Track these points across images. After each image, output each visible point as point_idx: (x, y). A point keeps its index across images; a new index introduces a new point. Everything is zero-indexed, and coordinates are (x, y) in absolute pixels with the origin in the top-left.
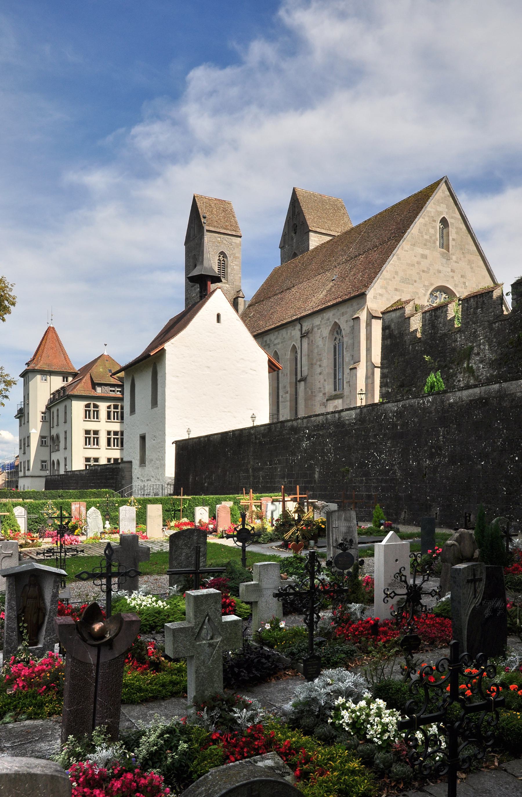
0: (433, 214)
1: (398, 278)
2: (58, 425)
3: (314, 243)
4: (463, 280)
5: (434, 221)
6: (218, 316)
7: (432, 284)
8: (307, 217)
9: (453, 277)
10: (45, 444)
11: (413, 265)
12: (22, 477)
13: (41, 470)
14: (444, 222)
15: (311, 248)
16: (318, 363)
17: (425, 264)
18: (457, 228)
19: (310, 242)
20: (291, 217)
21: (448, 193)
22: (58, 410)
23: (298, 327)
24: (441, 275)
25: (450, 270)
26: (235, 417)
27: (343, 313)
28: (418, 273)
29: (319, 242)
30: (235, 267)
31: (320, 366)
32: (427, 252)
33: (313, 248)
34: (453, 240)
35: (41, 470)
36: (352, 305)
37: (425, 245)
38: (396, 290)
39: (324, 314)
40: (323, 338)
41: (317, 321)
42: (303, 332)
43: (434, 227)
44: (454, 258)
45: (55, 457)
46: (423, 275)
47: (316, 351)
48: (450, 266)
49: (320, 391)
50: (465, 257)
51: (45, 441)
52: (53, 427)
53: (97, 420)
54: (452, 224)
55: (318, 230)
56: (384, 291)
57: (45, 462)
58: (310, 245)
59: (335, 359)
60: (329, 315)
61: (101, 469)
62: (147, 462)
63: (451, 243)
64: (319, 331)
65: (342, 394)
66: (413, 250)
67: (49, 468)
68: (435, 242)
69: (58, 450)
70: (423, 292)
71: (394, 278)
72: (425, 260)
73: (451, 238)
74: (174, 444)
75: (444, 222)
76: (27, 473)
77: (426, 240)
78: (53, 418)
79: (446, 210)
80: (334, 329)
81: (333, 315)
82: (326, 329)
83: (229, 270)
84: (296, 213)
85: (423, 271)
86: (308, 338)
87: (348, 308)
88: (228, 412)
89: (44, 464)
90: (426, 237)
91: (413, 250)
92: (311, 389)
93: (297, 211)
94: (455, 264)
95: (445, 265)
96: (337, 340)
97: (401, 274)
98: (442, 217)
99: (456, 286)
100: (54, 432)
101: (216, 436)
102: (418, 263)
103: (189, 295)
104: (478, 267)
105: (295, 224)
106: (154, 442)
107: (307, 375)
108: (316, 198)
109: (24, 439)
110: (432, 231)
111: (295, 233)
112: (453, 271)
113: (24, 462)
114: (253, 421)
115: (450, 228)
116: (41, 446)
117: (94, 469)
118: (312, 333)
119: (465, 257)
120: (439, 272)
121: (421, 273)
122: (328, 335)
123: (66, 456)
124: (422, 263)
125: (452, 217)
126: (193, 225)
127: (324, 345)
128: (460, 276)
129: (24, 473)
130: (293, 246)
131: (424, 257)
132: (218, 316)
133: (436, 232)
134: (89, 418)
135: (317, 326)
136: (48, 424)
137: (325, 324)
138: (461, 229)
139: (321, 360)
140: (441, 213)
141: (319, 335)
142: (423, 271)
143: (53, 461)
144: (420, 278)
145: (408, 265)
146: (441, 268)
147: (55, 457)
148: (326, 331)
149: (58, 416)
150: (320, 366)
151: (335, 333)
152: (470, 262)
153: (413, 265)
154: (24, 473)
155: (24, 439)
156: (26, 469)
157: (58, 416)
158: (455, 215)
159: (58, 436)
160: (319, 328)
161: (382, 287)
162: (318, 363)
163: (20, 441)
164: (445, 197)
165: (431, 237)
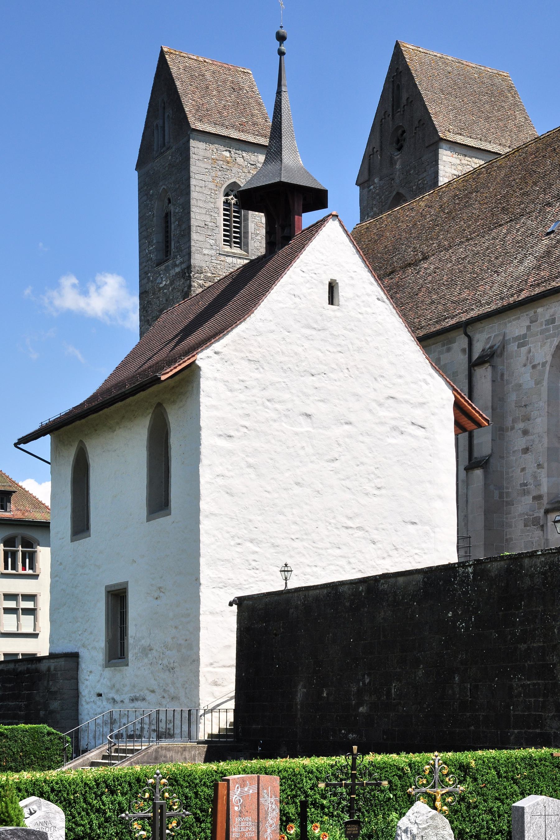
3: (448, 170)
8: (432, 109)
15: (443, 180)
16: (521, 425)
19: (441, 167)
23: (462, 342)
26: (374, 543)
29: (460, 168)
31: (525, 432)
33: (446, 180)
39: (540, 310)
40: (534, 367)
47: (513, 397)
55: (459, 139)
58: (441, 173)
74: (235, 607)
84: (404, 101)
86: (494, 367)
88: (359, 528)
93: (404, 96)
101: (401, 579)
105: (399, 127)
107: (490, 456)
108: (449, 69)
111: (400, 149)
114: (286, 579)
118: (502, 354)
137: (542, 332)
139: (527, 418)
160: (522, 341)
162: (521, 425)
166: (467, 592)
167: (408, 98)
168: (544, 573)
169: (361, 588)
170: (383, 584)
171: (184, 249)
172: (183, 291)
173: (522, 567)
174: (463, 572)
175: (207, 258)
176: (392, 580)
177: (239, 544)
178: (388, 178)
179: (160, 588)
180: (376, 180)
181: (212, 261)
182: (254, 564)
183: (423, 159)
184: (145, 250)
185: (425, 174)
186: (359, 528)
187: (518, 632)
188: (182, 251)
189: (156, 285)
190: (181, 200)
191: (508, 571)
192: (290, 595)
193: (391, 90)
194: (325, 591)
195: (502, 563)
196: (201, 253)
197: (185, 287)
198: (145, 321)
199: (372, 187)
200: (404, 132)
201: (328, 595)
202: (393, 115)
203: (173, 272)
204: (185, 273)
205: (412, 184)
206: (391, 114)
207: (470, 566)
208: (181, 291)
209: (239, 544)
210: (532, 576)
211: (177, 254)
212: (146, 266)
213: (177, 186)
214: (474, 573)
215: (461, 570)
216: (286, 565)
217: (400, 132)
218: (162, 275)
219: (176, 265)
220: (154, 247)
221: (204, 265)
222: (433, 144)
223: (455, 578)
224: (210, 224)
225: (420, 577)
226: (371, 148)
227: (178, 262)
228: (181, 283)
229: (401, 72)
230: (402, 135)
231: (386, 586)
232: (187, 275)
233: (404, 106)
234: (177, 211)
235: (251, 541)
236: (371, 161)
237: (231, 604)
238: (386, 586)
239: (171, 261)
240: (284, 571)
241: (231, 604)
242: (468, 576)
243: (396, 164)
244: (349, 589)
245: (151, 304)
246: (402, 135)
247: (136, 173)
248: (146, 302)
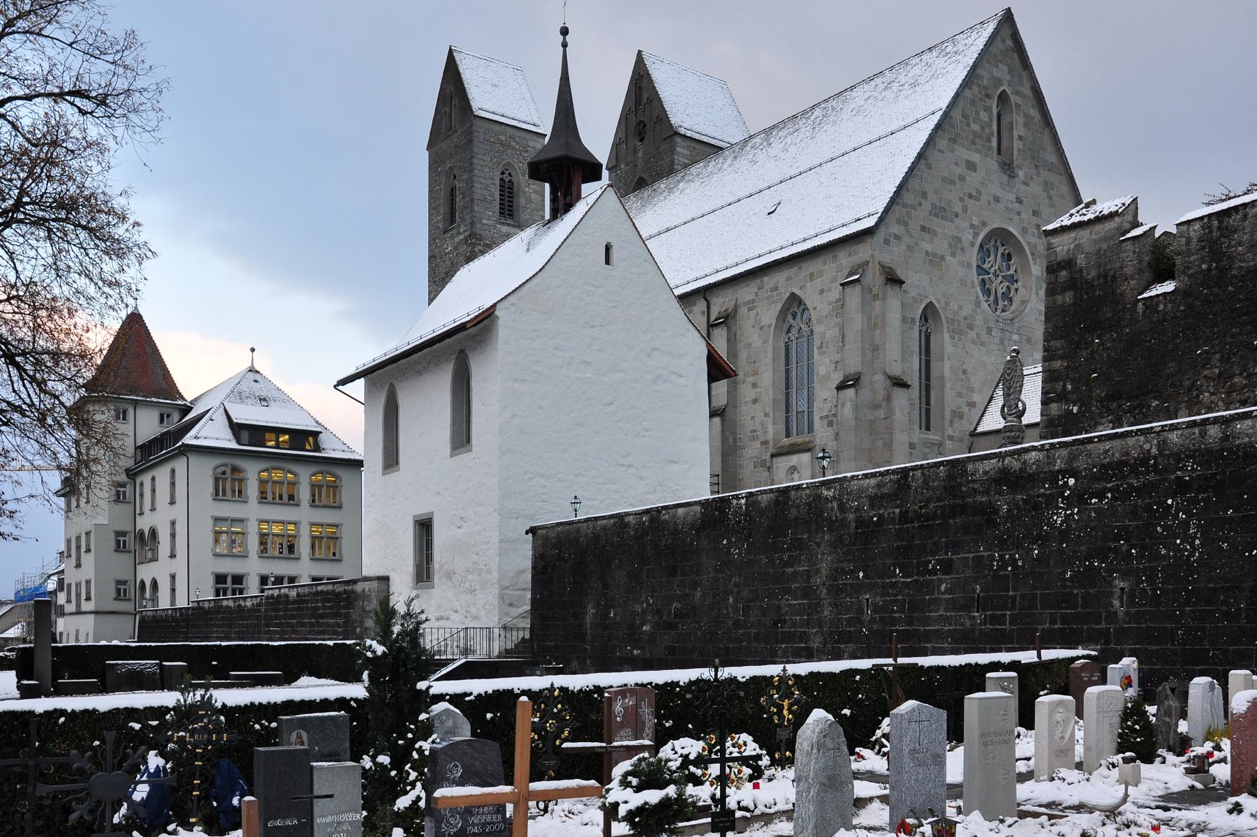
0: (985, 83)
1: (927, 206)
2: (153, 509)
4: (1035, 220)
5: (988, 96)
6: (608, 248)
7: (984, 224)
9: (1019, 213)
10: (124, 547)
11: (952, 182)
12: (72, 614)
13: (115, 599)
14: (1003, 97)
17: (973, 180)
18: (1026, 115)
20: (633, 109)
21: (1010, 43)
22: (153, 479)
24: (1000, 206)
25: (1013, 197)
27: (812, 275)
28: (961, 199)
30: (533, 196)
32: (976, 158)
34: (1020, 138)
35: (115, 599)
36: (835, 257)
37: (973, 143)
38: (924, 229)
41: (746, 293)
42: (713, 317)
43: (988, 109)
44: (1021, 174)
45: (146, 573)
46: (970, 203)
48: (1015, 190)
49: (754, 438)
50: (1038, 174)
51: (124, 541)
52: (142, 514)
53: (240, 499)
54: (1018, 106)
56: (902, 228)
57: (125, 583)
59: (787, 372)
60: (779, 278)
61: (298, 595)
62: (436, 578)
63: (1017, 145)
64: (753, 313)
65: (809, 442)
66: (952, 151)
67: (133, 597)
68: (989, 140)
69: (154, 559)
70: (970, 237)
71: (920, 204)
72: (974, 174)
73: (1016, 134)
74: (530, 535)
75: (1003, 97)
76: (86, 606)
77: (975, 133)
78: (142, 495)
79: (1008, 77)
80: (788, 310)
81: (788, 279)
82: (768, 310)
83: (522, 201)
84: (645, 100)
85: (970, 196)
87: (824, 263)
88: (630, 466)
89: (122, 587)
90: (975, 127)
91: (952, 151)
92: (734, 434)
93: (645, 95)
94: (1023, 187)
95: (1007, 189)
96: (794, 331)
97: (932, 197)
98: (1002, 89)
99: (1024, 231)
100: (144, 524)
101: (681, 511)
102: (962, 178)
103: (436, 251)
104: (1062, 196)
105: (641, 122)
106: (461, 531)
109: (78, 538)
110: (984, 116)
111: (641, 140)
112: (1019, 200)
113: (78, 585)
115: (1014, 115)
116: (116, 551)
117: (279, 596)
119: (1038, 174)
120: (997, 199)
121: (966, 199)
122: (774, 321)
123: (173, 571)
124: (968, 178)
125: (1018, 93)
126: (447, 109)
127: (765, 342)
128: (1030, 212)
129: (78, 605)
130: (636, 165)
131: (971, 166)
132: (608, 248)
133: (991, 120)
134: (224, 494)
135: (746, 303)
136: (129, 508)
138: (1032, 118)
140: (999, 82)
141: (751, 321)
142: (970, 196)
143: (143, 583)
144: (965, 210)
145: (944, 179)
146: (999, 193)
147: (146, 573)
148: (769, 315)
149: (153, 491)
150: (754, 385)
151: (790, 317)
152: (1047, 186)
153: (952, 182)
154: (78, 605)
155: (78, 538)
156: (83, 596)
157: (153, 491)
158: (1022, 89)
159: (153, 533)
161: (899, 222)
163: (69, 541)
164: (1007, 50)
165: (982, 128)
166: (740, 522)
167: (648, 98)
168: (809, 504)
169: (644, 519)
170: (664, 514)
173: (788, 498)
174: (737, 504)
176: (673, 511)
177: (531, 479)
179: (462, 518)
182: (544, 496)
185: (662, 162)
186: (630, 466)
187: (786, 557)
191: (777, 502)
192: (580, 524)
194: (612, 521)
195: (772, 495)
200: (645, 126)
201: (614, 524)
207: (743, 498)
209: (531, 479)
210: (798, 507)
214: (746, 504)
215: (735, 502)
216: (576, 497)
217: (642, 126)
223: (729, 508)
225: (698, 508)
230: (643, 128)
231: (667, 516)
235: (541, 476)
237: (527, 533)
238: (667, 516)
240: (574, 503)
241: (527, 533)
242: (741, 507)
244: (634, 519)
246: (643, 128)
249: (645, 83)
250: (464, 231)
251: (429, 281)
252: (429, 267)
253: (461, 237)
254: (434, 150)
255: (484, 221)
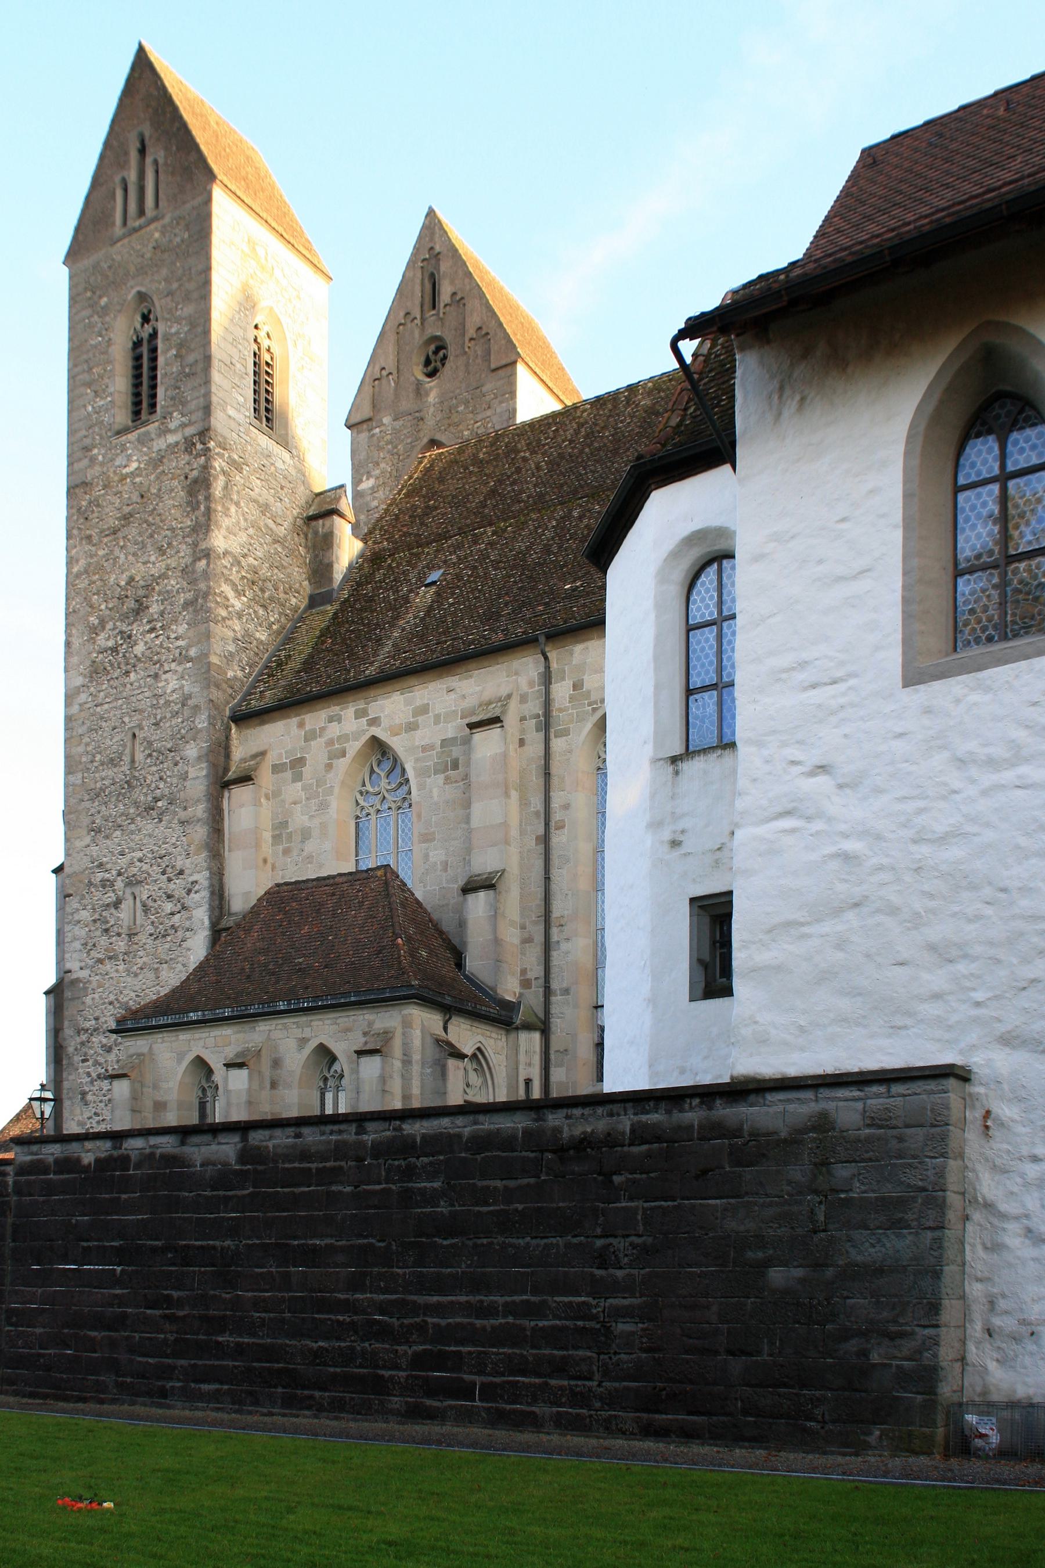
93: (446, 292)
167: (454, 294)
171: (192, 400)
172: (186, 478)
175: (233, 425)
178: (410, 418)
180: (386, 420)
181: (241, 434)
183: (484, 389)
184: (85, 406)
185: (489, 413)
188: (184, 403)
189: (112, 470)
190: (185, 309)
193: (418, 281)
196: (224, 411)
197: (192, 470)
198: (81, 539)
199: (377, 430)
202: (422, 318)
203: (160, 444)
204: (194, 444)
205: (461, 427)
206: (418, 317)
208: (182, 478)
211: (170, 409)
212: (85, 437)
213: (175, 286)
217: (432, 347)
218: (130, 452)
219: (164, 432)
220: (109, 399)
221: (228, 436)
222: (506, 366)
224: (238, 366)
226: (377, 368)
227: (172, 426)
228: (183, 462)
229: (439, 253)
232: (199, 446)
233: (446, 306)
234: (173, 330)
236: (377, 389)
239: (157, 424)
243: (427, 394)
245: (98, 506)
247: (65, 270)
248: (84, 503)
249: (444, 266)
250: (183, 426)
251: (69, 537)
252: (69, 507)
253: (171, 439)
254: (87, 262)
255: (231, 412)
